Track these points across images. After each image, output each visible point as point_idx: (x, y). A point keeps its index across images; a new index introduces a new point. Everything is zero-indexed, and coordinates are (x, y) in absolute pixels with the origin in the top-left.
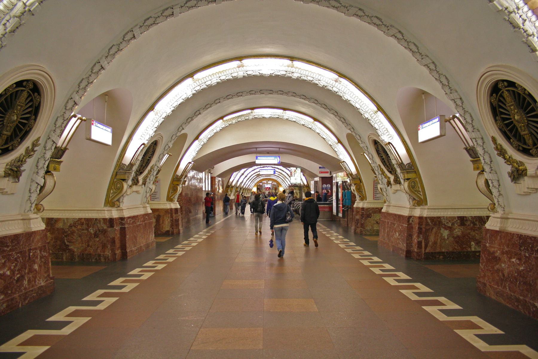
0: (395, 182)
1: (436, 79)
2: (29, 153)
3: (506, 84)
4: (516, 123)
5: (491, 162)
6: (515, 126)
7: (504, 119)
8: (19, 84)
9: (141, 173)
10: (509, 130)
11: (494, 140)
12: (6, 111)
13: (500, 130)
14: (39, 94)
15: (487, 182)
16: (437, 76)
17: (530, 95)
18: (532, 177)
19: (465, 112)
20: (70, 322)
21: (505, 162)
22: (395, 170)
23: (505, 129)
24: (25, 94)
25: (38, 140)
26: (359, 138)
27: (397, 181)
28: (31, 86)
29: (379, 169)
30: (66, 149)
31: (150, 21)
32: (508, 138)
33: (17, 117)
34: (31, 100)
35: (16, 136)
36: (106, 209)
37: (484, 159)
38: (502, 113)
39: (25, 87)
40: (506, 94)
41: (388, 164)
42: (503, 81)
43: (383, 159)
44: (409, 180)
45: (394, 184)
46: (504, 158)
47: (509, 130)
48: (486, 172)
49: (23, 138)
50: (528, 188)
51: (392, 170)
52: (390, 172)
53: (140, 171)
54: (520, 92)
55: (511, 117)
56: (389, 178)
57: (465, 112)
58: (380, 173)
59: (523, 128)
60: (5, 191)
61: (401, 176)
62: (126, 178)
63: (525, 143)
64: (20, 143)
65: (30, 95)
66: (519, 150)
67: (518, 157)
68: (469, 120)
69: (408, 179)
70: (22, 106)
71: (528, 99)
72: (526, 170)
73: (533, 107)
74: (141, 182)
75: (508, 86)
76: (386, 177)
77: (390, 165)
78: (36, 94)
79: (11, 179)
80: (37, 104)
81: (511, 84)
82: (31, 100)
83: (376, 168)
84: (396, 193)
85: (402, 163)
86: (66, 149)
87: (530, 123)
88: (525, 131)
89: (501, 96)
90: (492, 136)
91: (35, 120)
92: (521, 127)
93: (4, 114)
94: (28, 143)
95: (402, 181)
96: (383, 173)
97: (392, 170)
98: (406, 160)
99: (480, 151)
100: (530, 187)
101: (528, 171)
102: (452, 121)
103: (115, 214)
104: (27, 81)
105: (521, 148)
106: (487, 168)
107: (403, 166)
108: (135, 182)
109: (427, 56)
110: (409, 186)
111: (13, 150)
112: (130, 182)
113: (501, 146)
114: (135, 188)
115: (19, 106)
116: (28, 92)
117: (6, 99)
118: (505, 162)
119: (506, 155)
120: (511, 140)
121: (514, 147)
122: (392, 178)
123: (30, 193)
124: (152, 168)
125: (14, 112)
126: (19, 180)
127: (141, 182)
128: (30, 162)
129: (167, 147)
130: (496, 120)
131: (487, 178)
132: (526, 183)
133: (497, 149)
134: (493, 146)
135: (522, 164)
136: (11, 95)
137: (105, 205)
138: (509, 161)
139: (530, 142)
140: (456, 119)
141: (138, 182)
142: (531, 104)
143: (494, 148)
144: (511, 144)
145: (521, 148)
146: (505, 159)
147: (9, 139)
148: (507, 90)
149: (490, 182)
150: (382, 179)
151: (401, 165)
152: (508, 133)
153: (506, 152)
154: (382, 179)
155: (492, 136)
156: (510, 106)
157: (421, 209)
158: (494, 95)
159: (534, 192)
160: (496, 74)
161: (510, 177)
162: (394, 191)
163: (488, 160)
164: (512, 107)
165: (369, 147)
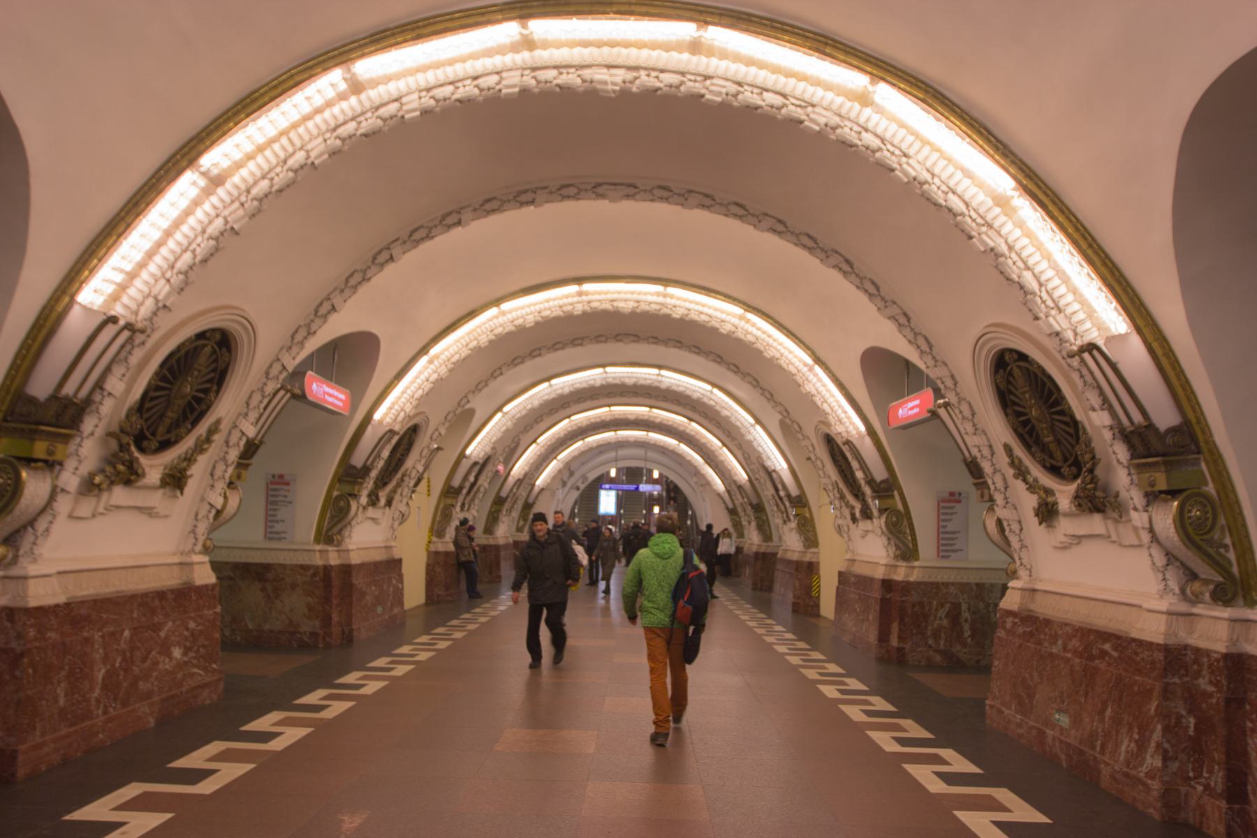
0: (862, 516)
1: (910, 341)
2: (199, 448)
3: (1016, 356)
4: (1034, 421)
5: (1006, 488)
7: (1019, 414)
8: (201, 336)
9: (385, 484)
10: (1027, 432)
11: (1008, 450)
12: (175, 377)
13: (1015, 431)
14: (229, 350)
15: (999, 522)
16: (911, 336)
17: (1050, 378)
18: (1066, 515)
20: (280, 734)
21: (1027, 489)
23: (1020, 430)
24: (208, 350)
25: (218, 422)
27: (867, 515)
28: (218, 337)
29: (836, 490)
30: (261, 442)
31: (422, 233)
32: (1027, 446)
33: (191, 389)
34: (216, 361)
35: (185, 418)
36: (318, 547)
37: (995, 482)
38: (1015, 404)
39: (208, 339)
40: (1016, 372)
41: (851, 480)
42: (1011, 351)
43: (843, 471)
44: (888, 512)
46: (1025, 480)
47: (1027, 432)
48: (997, 506)
49: (195, 423)
50: (1065, 535)
53: (382, 481)
54: (1036, 371)
58: (838, 495)
59: (1045, 432)
60: (155, 511)
61: (874, 505)
62: (356, 492)
63: (1051, 456)
64: (189, 431)
65: (214, 352)
66: (1044, 467)
67: (1047, 480)
69: (886, 510)
70: (199, 371)
71: (1049, 384)
72: (1056, 503)
73: (1056, 399)
74: (383, 501)
75: (1018, 360)
76: (848, 505)
78: (224, 350)
79: (168, 490)
80: (224, 366)
81: (1022, 357)
82: (216, 361)
83: (830, 487)
86: (261, 442)
87: (1056, 423)
88: (1048, 436)
89: (1010, 374)
90: (1005, 443)
91: (218, 392)
92: (1042, 429)
93: (170, 383)
94: (202, 429)
95: (875, 512)
96: (842, 497)
97: (858, 494)
98: (880, 474)
99: (986, 467)
100: (1068, 533)
101: (1060, 504)
103: (334, 559)
104: (214, 330)
105: (1048, 465)
106: (999, 498)
107: (874, 485)
108: (373, 500)
109: (894, 303)
110: (886, 523)
111: (176, 442)
112: (364, 500)
113: (1020, 460)
114: (371, 512)
115: (196, 370)
116: (213, 347)
117: (178, 361)
118: (1027, 489)
119: (1029, 476)
120: (1033, 449)
121: (1037, 462)
123: (197, 520)
124: (404, 476)
125: (187, 380)
126: (182, 494)
127: (383, 501)
128: (202, 462)
129: (436, 434)
130: (1006, 415)
131: (1001, 517)
132: (1066, 526)
133: (1012, 464)
134: (1007, 460)
135: (1049, 492)
136: (187, 354)
137: (317, 540)
138: (1032, 487)
139: (1058, 455)
141: (378, 499)
142: (1053, 394)
143: (1009, 464)
144: (1033, 455)
145: (1048, 465)
146: (1027, 483)
147: (176, 424)
148: (1019, 367)
149: (1005, 524)
150: (841, 507)
151: (871, 481)
152: (1026, 436)
154: (841, 507)
155: (1005, 443)
156: (1024, 393)
157: (906, 567)
158: (1001, 371)
159: (1075, 542)
160: (1002, 338)
161: (1037, 515)
163: (1000, 485)
164: (1027, 395)
165: (816, 446)
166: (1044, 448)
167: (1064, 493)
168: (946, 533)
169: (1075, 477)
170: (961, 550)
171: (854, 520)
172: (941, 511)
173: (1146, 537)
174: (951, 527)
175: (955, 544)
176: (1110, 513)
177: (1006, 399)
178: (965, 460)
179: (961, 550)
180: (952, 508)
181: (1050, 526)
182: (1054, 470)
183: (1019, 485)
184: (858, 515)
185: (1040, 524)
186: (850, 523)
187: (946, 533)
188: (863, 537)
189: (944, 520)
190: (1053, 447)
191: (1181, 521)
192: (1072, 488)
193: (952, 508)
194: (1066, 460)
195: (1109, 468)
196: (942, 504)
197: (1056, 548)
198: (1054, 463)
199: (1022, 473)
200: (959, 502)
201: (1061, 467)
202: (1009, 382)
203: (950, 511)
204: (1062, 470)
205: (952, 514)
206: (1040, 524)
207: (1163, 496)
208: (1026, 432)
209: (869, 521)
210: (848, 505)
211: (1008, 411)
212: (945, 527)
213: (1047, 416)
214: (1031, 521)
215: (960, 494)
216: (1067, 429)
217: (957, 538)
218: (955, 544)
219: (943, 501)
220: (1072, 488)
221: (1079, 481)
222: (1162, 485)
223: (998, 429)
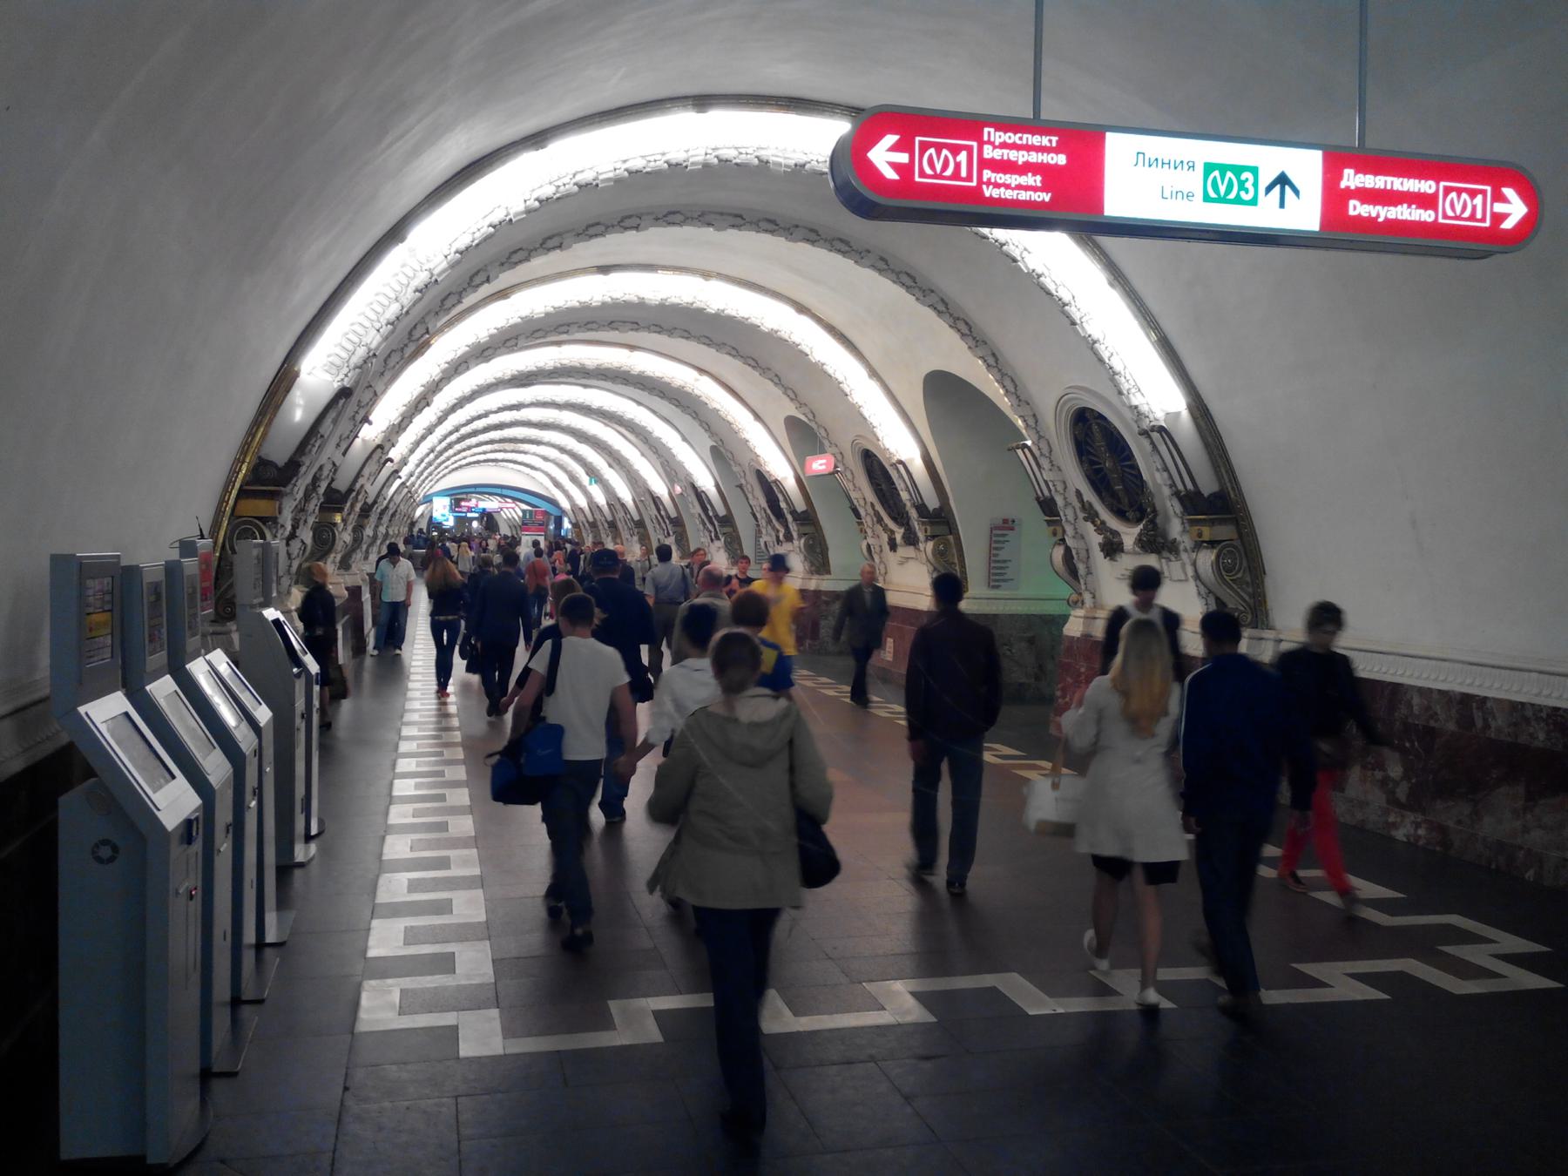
6: (1106, 474)
19: (1040, 437)
22: (907, 516)
26: (824, 434)
27: (911, 540)
38: (1089, 453)
40: (1095, 427)
43: (881, 490)
44: (936, 539)
45: (901, 546)
46: (1093, 523)
51: (899, 516)
52: (894, 519)
55: (1102, 461)
56: (892, 532)
57: (1040, 437)
67: (1113, 523)
68: (1045, 451)
76: (886, 528)
77: (895, 504)
84: (906, 565)
85: (924, 505)
87: (1126, 475)
96: (880, 520)
102: (1019, 452)
113: (1090, 505)
122: (899, 534)
135: (1116, 533)
138: (1102, 528)
140: (1026, 450)
145: (1115, 509)
146: (1095, 526)
148: (1098, 424)
153: (1097, 514)
161: (1102, 550)
162: (900, 559)
163: (1071, 518)
164: (1102, 449)
166: (1114, 495)
167: (1129, 535)
168: (999, 561)
169: (1139, 521)
170: (1012, 580)
171: (893, 546)
172: (994, 539)
173: (1190, 571)
174: (1003, 555)
175: (1005, 574)
176: (1165, 554)
177: (1082, 448)
178: (1038, 499)
179: (1012, 580)
180: (1004, 535)
181: (1112, 559)
182: (1120, 514)
183: (1090, 527)
184: (898, 537)
185: (1105, 558)
186: (886, 548)
187: (999, 561)
188: (901, 564)
189: (996, 549)
190: (1121, 494)
191: (1217, 564)
192: (1136, 530)
193: (1004, 535)
194: (1131, 506)
195: (1167, 519)
196: (994, 532)
197: (1119, 579)
198: (1121, 506)
199: (1091, 516)
200: (1012, 529)
201: (1126, 512)
202: (1087, 435)
203: (1001, 539)
204: (1127, 514)
205: (1004, 542)
206: (1105, 558)
207: (1205, 544)
208: (1098, 480)
209: (912, 548)
210: (886, 528)
211: (1084, 458)
212: (995, 555)
213: (1119, 468)
214: (1098, 555)
215: (1013, 521)
216: (1135, 480)
217: (1007, 567)
218: (1005, 574)
219: (997, 528)
220: (1136, 530)
221: (1141, 526)
222: (1206, 537)
223: (1076, 479)
